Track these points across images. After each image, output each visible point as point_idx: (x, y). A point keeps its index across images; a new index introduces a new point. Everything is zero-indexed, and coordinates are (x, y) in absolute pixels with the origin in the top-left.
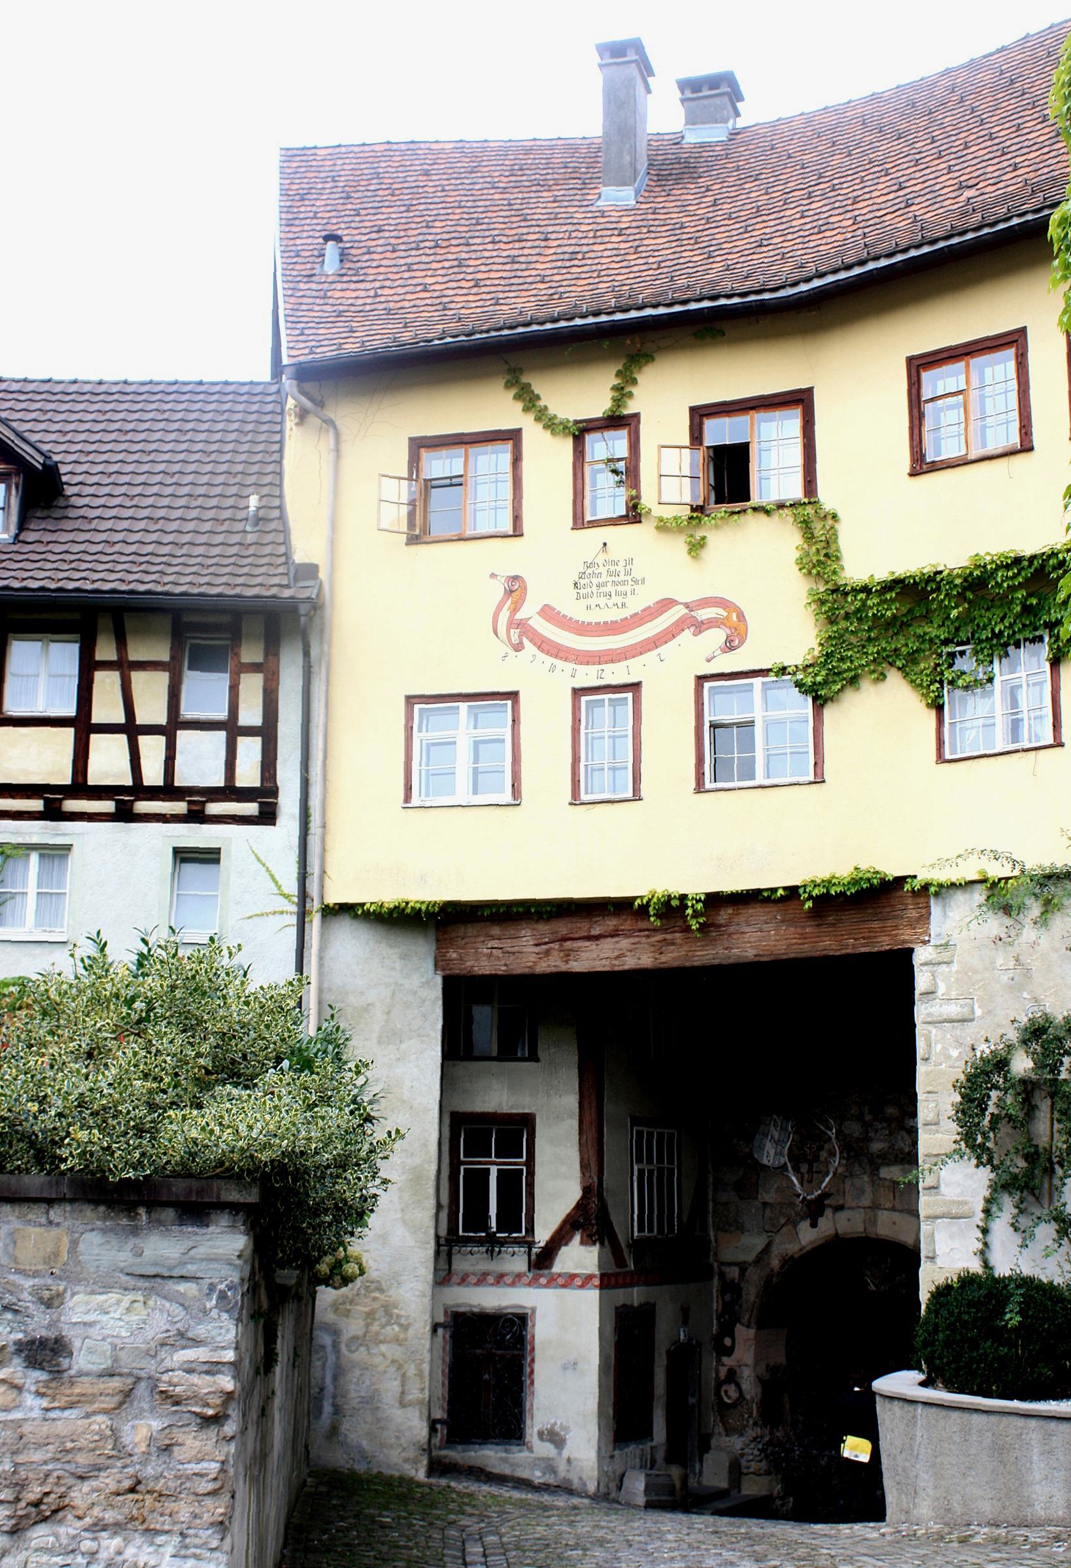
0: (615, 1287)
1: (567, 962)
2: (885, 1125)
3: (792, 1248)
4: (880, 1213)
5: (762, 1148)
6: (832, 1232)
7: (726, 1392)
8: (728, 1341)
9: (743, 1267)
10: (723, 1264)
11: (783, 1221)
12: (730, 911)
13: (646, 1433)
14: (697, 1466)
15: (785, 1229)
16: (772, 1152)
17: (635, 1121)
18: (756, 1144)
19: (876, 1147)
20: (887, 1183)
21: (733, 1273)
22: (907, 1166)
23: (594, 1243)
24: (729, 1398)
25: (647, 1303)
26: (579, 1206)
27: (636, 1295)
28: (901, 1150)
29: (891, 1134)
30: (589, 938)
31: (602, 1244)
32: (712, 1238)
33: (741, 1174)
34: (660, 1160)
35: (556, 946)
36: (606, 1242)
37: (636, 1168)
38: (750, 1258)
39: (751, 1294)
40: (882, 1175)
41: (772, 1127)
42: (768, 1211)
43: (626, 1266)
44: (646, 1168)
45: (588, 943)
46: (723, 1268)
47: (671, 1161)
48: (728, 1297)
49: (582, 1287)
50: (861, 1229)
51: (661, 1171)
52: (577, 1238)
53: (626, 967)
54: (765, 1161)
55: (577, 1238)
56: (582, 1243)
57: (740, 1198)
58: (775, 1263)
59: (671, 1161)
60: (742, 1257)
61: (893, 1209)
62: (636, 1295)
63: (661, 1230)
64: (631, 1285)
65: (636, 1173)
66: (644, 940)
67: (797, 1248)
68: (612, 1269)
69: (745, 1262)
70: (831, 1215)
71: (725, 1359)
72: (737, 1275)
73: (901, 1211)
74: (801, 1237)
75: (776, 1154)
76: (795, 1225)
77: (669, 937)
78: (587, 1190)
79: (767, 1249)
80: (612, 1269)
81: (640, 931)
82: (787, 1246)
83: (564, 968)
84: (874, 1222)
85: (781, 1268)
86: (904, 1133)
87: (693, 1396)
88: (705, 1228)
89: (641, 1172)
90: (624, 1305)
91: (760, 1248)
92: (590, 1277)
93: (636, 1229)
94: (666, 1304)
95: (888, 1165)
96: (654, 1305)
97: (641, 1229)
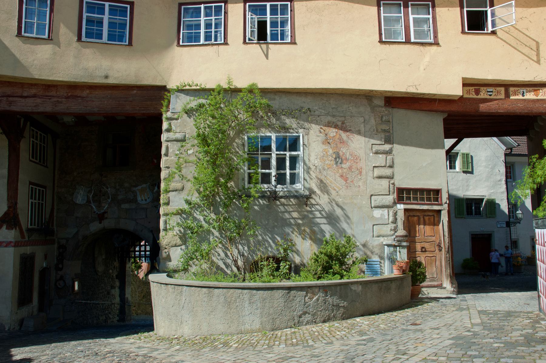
0: (20, 246)
1: (10, 106)
8: (60, 266)
12: (88, 92)
13: (30, 301)
17: (31, 183)
19: (120, 197)
23: (12, 229)
26: (6, 214)
27: (28, 250)
30: (22, 97)
31: (16, 229)
32: (55, 230)
34: (39, 200)
35: (5, 99)
37: (30, 201)
44: (34, 201)
45: (20, 99)
47: (42, 200)
48: (61, 250)
49: (6, 246)
51: (39, 203)
52: (4, 227)
53: (39, 111)
54: (78, 202)
55: (4, 227)
56: (7, 228)
59: (42, 200)
63: (38, 226)
64: (26, 246)
66: (48, 100)
68: (20, 239)
77: (60, 100)
78: (9, 207)
80: (20, 239)
81: (47, 96)
83: (8, 108)
88: (53, 225)
89: (32, 203)
90: (24, 254)
92: (11, 242)
93: (29, 224)
94: (39, 252)
97: (31, 225)
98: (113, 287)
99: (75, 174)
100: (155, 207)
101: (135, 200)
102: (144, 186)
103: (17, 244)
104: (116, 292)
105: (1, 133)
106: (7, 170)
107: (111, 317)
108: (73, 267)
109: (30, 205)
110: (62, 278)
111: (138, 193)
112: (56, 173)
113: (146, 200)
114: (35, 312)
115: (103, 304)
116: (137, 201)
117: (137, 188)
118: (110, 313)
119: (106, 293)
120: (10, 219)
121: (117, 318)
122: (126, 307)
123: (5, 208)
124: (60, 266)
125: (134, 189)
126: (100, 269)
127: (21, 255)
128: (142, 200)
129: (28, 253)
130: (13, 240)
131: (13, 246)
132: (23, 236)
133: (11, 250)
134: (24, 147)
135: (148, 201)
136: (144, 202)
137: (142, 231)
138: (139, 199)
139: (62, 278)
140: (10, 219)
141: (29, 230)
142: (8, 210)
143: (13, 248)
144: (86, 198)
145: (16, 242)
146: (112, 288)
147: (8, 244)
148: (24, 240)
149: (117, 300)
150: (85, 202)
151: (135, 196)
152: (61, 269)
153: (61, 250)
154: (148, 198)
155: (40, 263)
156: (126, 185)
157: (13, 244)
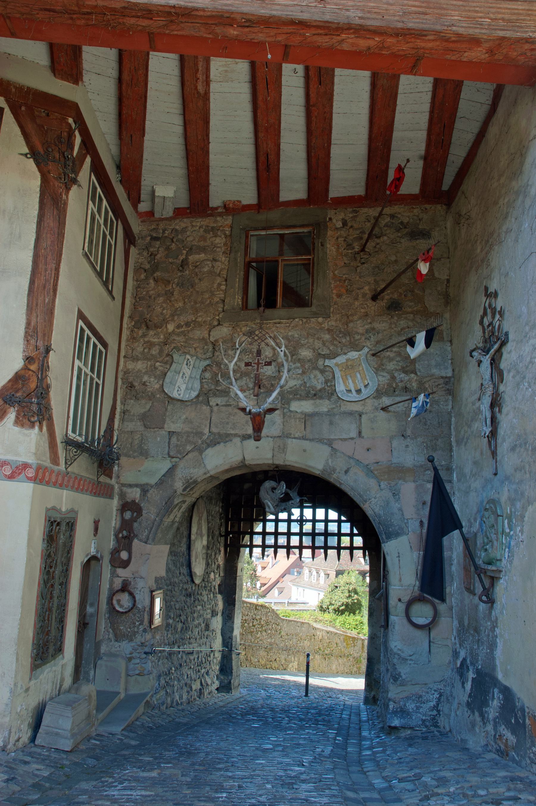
0: (48, 483)
2: (298, 365)
3: (198, 473)
4: (289, 441)
5: (173, 383)
6: (239, 458)
7: (119, 601)
8: (124, 555)
9: (145, 489)
10: (123, 485)
11: (189, 448)
14: (92, 673)
15: (190, 455)
16: (183, 387)
18: (167, 380)
20: (299, 416)
21: (135, 494)
22: (318, 401)
23: (32, 426)
24: (121, 606)
25: (72, 511)
26: (18, 378)
27: (64, 499)
28: (314, 388)
29: (304, 373)
31: (41, 429)
33: (148, 407)
36: (45, 428)
38: (153, 481)
39: (150, 512)
40: (292, 409)
41: (185, 365)
42: (174, 440)
43: (58, 464)
46: (124, 489)
48: (128, 515)
50: (270, 456)
52: (12, 416)
54: (175, 395)
55: (12, 416)
56: (18, 422)
57: (145, 426)
58: (179, 485)
60: (144, 480)
61: (304, 438)
62: (64, 499)
65: (76, 368)
67: (201, 471)
69: (147, 484)
70: (239, 444)
71: (120, 571)
72: (138, 496)
73: (311, 440)
74: (206, 462)
75: (187, 389)
76: (201, 451)
78: (29, 360)
79: (171, 471)
82: (192, 470)
84: (283, 449)
85: (184, 490)
86: (317, 373)
87: (92, 605)
90: (54, 509)
91: (163, 472)
92: (26, 466)
95: (299, 399)
96: (76, 513)
97: (74, 431)
98: (214, 613)
99: (171, 327)
100: (383, 409)
101: (328, 392)
102: (353, 355)
103: (41, 477)
104: (217, 623)
105: (26, 155)
106: (31, 254)
107: (209, 682)
108: (151, 561)
109: (75, 373)
110: (125, 588)
111: (338, 374)
112: (125, 326)
113: (359, 391)
114: (68, 681)
115: (198, 652)
116: (334, 392)
117: (334, 361)
118: (207, 673)
119: (203, 625)
120: (26, 398)
121: (217, 684)
122: (234, 656)
123: (17, 364)
124: (124, 555)
125: (327, 362)
126: (198, 569)
127: (48, 510)
128: (349, 391)
129: (64, 509)
130: (31, 460)
131: (30, 479)
132: (55, 460)
133: (24, 490)
134: (78, 202)
135: (365, 392)
136: (354, 396)
137: (346, 472)
138: (340, 387)
139: (125, 588)
140: (26, 398)
141: (68, 442)
142: (26, 368)
143: (31, 485)
144: (197, 385)
145: (39, 468)
146: (212, 616)
147: (17, 472)
148: (56, 468)
149: (218, 644)
150: (194, 394)
151: (330, 381)
152: (125, 564)
153: (128, 515)
154: (366, 386)
155: (84, 545)
156: (305, 353)
157: (31, 473)
